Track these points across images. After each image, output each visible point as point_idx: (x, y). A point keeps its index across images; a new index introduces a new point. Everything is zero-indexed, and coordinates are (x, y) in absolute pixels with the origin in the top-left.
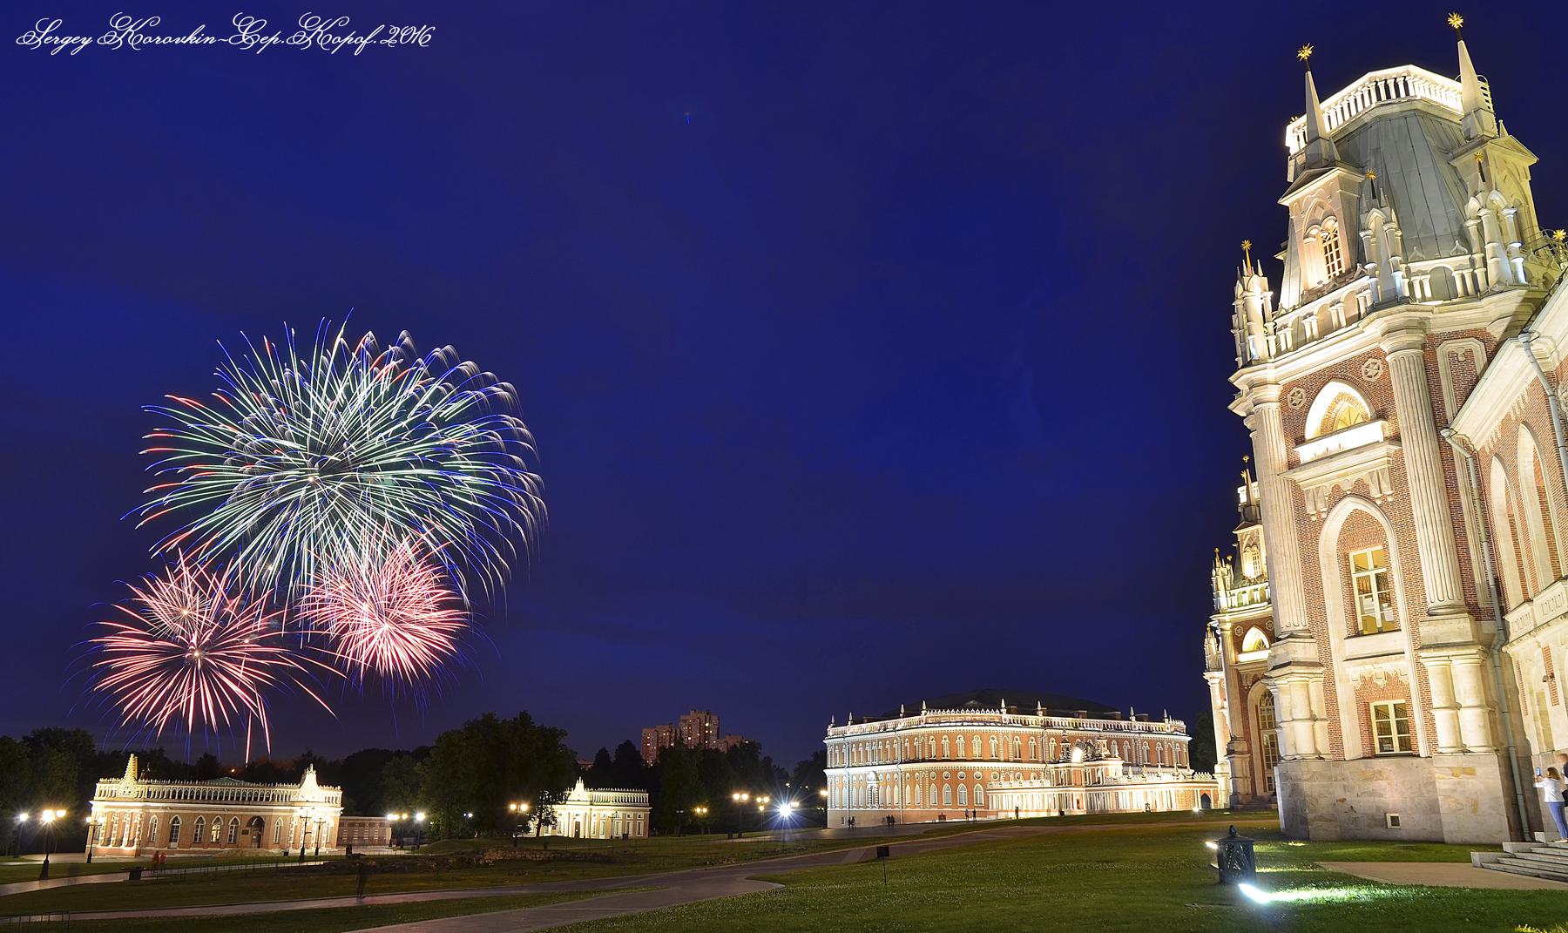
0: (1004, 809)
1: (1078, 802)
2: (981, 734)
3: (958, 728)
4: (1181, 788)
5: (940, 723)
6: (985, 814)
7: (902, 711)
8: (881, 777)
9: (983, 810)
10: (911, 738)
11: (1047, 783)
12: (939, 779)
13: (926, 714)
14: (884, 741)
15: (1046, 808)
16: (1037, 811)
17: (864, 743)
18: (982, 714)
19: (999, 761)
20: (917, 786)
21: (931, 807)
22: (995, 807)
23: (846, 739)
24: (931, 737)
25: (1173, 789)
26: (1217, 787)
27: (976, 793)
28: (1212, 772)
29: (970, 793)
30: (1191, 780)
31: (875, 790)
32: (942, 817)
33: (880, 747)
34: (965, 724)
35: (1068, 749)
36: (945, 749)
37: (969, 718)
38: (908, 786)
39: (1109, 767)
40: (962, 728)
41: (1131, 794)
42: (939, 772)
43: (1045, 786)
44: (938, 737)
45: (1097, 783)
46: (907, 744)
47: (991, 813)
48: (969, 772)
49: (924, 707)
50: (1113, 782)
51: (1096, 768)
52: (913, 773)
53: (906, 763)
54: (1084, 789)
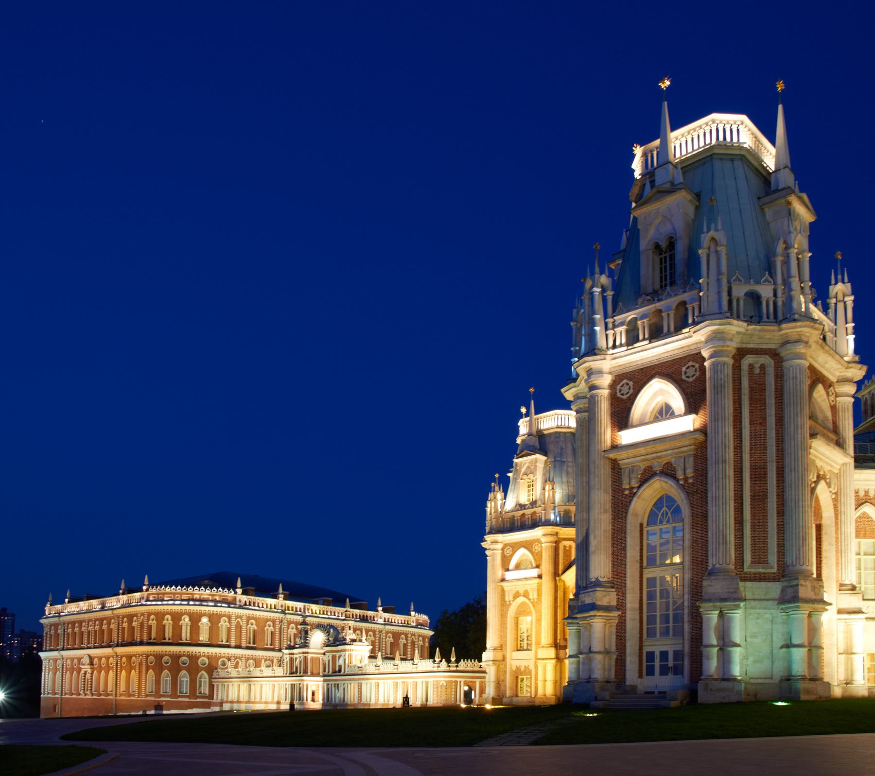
0: (230, 699)
1: (313, 694)
2: (211, 616)
3: (183, 608)
4: (443, 678)
5: (163, 600)
6: (208, 705)
7: (123, 586)
8: (96, 661)
9: (206, 700)
10: (130, 617)
11: (279, 671)
12: (158, 665)
13: (147, 590)
14: (101, 620)
15: (276, 700)
16: (266, 703)
17: (81, 622)
18: (201, 592)
19: (229, 646)
20: (133, 671)
21: (147, 696)
22: (220, 698)
23: (62, 619)
24: (152, 617)
25: (431, 679)
26: (484, 677)
27: (200, 682)
28: (480, 660)
29: (193, 682)
30: (455, 669)
31: (88, 676)
32: (159, 707)
33: (97, 628)
34: (191, 603)
35: (306, 632)
36: (167, 631)
37: (197, 596)
38: (124, 672)
39: (354, 653)
40: (188, 608)
41: (378, 685)
42: (159, 657)
43: (276, 675)
44: (160, 616)
45: (337, 672)
46: (125, 625)
47: (216, 704)
48: (194, 658)
49: (146, 582)
50: (357, 671)
51: (338, 654)
52: (129, 657)
53: (123, 645)
54: (322, 679)
